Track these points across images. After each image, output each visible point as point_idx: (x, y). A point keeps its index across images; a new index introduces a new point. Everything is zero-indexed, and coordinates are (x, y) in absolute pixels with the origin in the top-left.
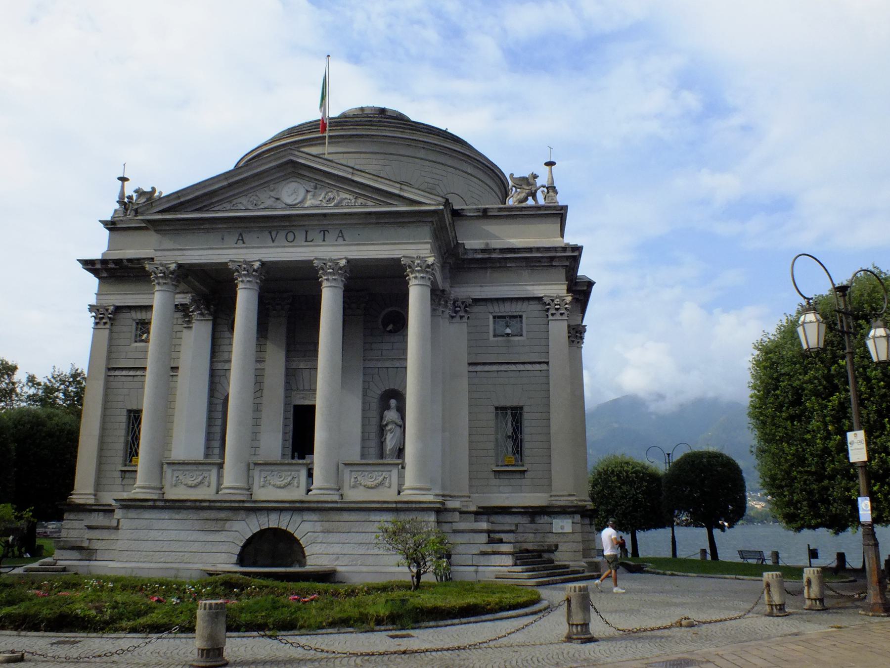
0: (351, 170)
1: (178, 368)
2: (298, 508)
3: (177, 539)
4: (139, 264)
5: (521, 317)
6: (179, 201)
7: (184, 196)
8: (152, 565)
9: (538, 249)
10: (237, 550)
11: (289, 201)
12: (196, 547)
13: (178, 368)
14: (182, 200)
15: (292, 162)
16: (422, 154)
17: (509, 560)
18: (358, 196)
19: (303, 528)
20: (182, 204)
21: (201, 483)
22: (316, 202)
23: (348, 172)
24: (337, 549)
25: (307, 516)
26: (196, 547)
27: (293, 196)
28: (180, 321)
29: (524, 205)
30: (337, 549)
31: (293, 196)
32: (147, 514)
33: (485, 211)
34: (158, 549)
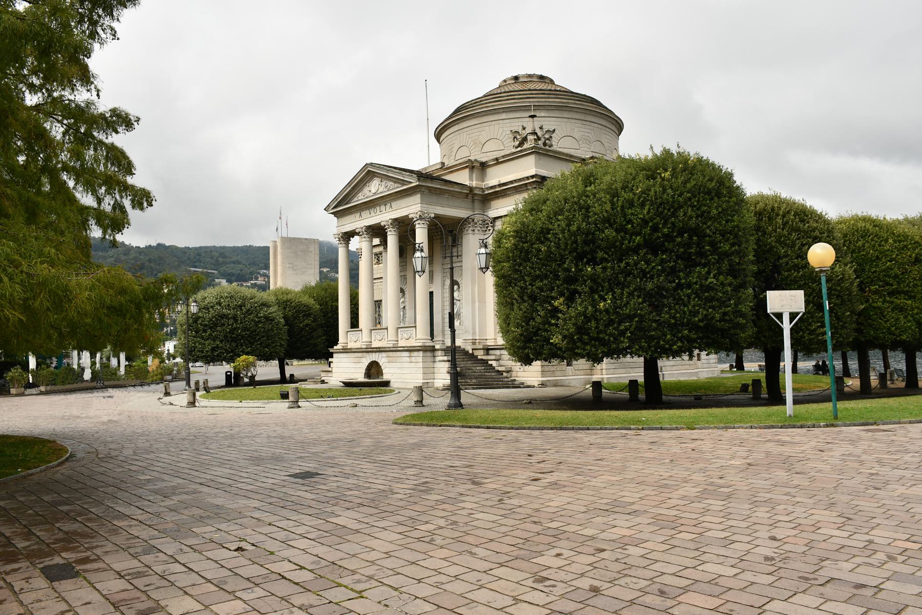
2: (379, 350)
9: (515, 181)
11: (373, 191)
15: (369, 171)
16: (504, 116)
18: (395, 182)
19: (381, 359)
20: (339, 202)
22: (381, 189)
24: (392, 371)
25: (384, 354)
27: (375, 188)
29: (526, 146)
30: (392, 371)
31: (375, 188)
33: (497, 159)
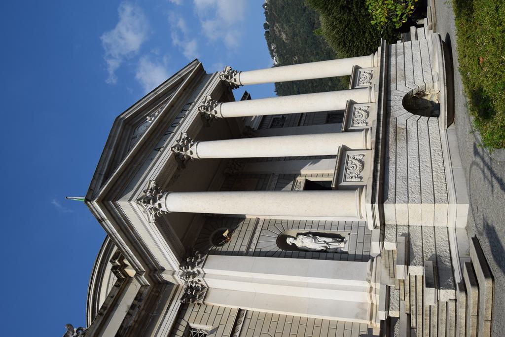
0: (153, 93)
1: (240, 310)
3: (417, 157)
4: (125, 329)
5: (274, 119)
6: (103, 175)
7: (102, 171)
8: (448, 170)
10: (424, 119)
12: (424, 142)
13: (240, 310)
14: (104, 173)
17: (420, 30)
21: (360, 161)
23: (152, 96)
26: (424, 142)
28: (197, 307)
32: (391, 182)
34: (429, 170)
